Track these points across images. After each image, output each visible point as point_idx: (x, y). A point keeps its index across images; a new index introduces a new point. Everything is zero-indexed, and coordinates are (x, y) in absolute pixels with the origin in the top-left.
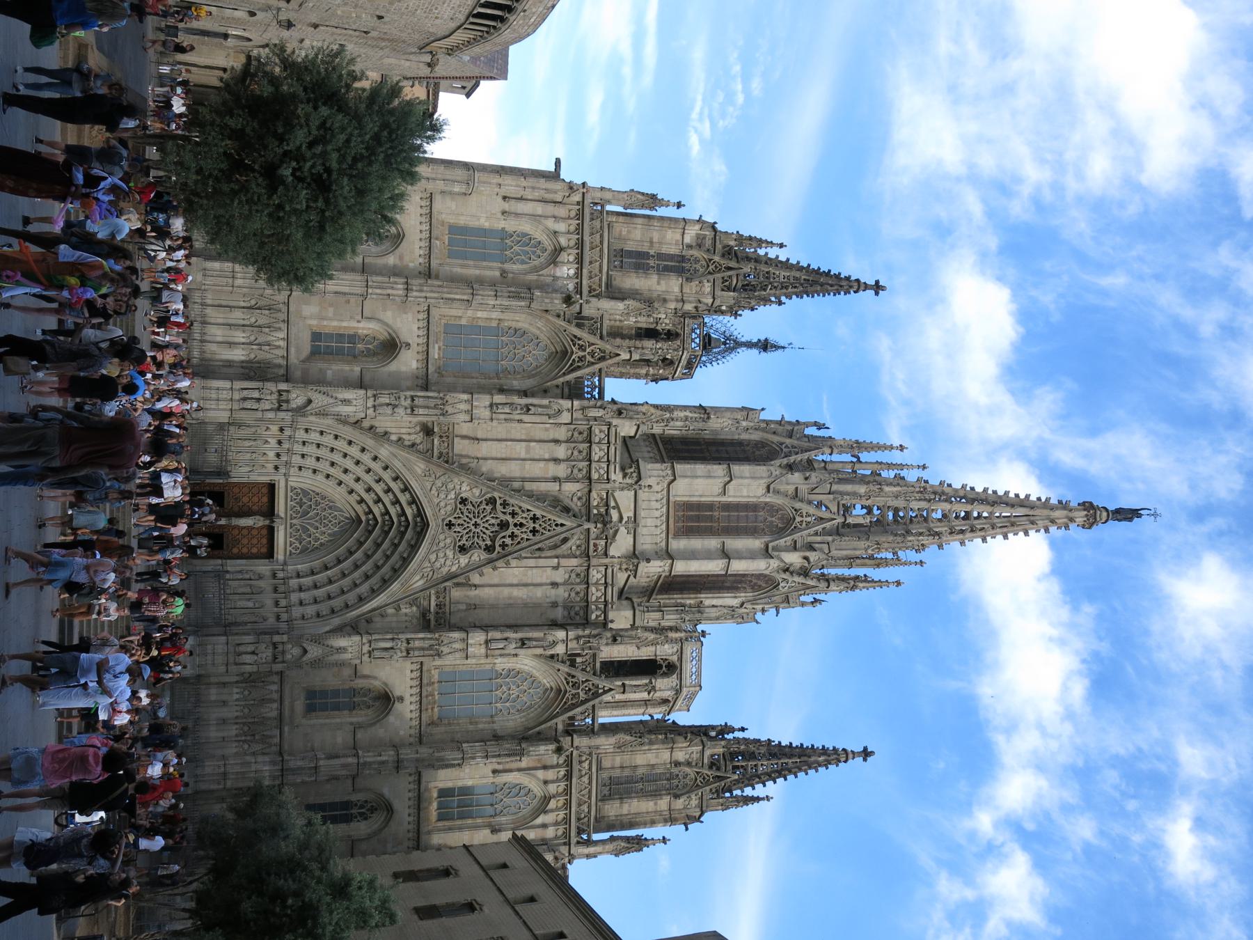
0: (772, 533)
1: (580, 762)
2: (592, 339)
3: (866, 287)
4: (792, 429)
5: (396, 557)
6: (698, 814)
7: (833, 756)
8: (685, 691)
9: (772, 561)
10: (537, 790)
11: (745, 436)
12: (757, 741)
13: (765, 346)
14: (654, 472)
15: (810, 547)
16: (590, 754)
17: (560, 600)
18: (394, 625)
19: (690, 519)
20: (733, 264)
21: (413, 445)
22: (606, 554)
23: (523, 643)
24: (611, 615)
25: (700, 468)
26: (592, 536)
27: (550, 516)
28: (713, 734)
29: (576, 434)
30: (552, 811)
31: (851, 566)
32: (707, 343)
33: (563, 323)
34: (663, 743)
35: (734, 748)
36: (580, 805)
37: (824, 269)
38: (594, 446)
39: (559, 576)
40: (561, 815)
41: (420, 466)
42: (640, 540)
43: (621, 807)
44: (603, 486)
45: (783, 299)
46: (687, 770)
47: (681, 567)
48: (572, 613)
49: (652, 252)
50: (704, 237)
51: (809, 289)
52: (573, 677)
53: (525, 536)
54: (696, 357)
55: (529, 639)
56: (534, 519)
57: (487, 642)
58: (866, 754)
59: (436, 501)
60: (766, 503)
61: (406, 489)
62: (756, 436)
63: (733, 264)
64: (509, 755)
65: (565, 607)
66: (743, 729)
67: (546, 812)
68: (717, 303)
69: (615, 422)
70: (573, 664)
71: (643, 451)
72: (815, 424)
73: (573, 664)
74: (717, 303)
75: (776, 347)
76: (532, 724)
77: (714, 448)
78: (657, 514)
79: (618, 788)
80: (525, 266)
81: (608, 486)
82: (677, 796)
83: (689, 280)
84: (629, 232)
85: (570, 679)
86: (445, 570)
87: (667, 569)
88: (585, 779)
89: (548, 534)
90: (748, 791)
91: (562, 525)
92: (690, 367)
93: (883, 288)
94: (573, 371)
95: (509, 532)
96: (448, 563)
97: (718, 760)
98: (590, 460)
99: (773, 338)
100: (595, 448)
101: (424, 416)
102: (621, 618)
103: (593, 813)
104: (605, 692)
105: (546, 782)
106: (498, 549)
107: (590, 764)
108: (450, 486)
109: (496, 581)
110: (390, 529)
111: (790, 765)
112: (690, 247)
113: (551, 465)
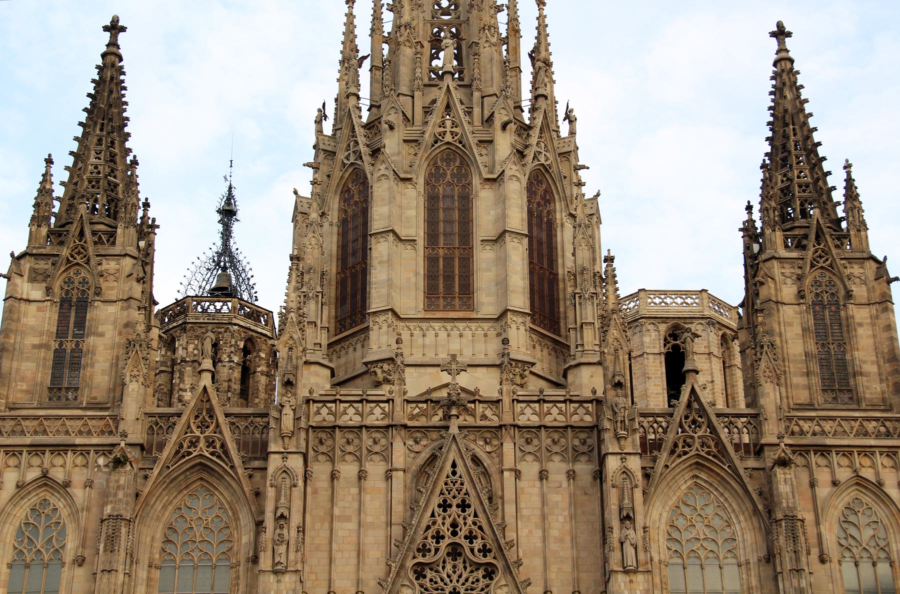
0: (467, 175)
1: (802, 433)
2: (178, 428)
3: (113, 43)
4: (325, 152)
6: (874, 265)
7: (785, 76)
8: (707, 313)
9: (508, 173)
10: (847, 497)
11: (334, 216)
12: (766, 184)
13: (228, 213)
14: (380, 341)
15: (489, 121)
16: (790, 419)
17: (564, 467)
19: (449, 289)
20: (74, 229)
22: (498, 401)
23: (627, 518)
24: (587, 394)
25: (378, 275)
26: (470, 421)
27: (441, 484)
28: (756, 248)
29: (323, 449)
30: (877, 474)
31: (518, 70)
32: (223, 292)
33: (156, 471)
34: (770, 315)
35: (775, 216)
36: (866, 434)
37: (87, 103)
38: (340, 422)
39: (530, 468)
40: (879, 459)
42: (481, 359)
43: (867, 375)
44: (398, 408)
45: (129, 159)
46: (808, 281)
47: (520, 300)
48: (585, 449)
49: (54, 345)
50: (33, 270)
51: (116, 123)
52: (676, 445)
53: (470, 520)
54: (242, 308)
55: (621, 510)
56: (445, 506)
57: (626, 572)
58: (781, 33)
60: (427, 183)
62: (334, 204)
63: (74, 229)
64: (795, 539)
65: (575, 460)
66: (749, 208)
67: (880, 485)
68: (135, 252)
69: (303, 392)
70: (657, 445)
71: (353, 359)
72: (319, 122)
73: (657, 445)
74: (135, 252)
75: (230, 198)
76: (749, 505)
77: (351, 261)
78: (443, 334)
79: (837, 378)
80: (70, 529)
81: (398, 401)
82: (849, 295)
83: (98, 292)
84: (23, 379)
85: (680, 450)
87: (520, 320)
88: (828, 426)
89: (467, 486)
90: (838, 196)
91: (454, 465)
92: (256, 314)
93: (115, 22)
94: (226, 452)
95: (465, 544)
97: (794, 237)
98: (361, 427)
99: (218, 202)
100: (343, 421)
102: (589, 381)
103: (878, 414)
104: (698, 399)
105: (835, 483)
107: (805, 419)
109: (538, 562)
111: (799, 137)
112: (48, 290)
113: (368, 484)
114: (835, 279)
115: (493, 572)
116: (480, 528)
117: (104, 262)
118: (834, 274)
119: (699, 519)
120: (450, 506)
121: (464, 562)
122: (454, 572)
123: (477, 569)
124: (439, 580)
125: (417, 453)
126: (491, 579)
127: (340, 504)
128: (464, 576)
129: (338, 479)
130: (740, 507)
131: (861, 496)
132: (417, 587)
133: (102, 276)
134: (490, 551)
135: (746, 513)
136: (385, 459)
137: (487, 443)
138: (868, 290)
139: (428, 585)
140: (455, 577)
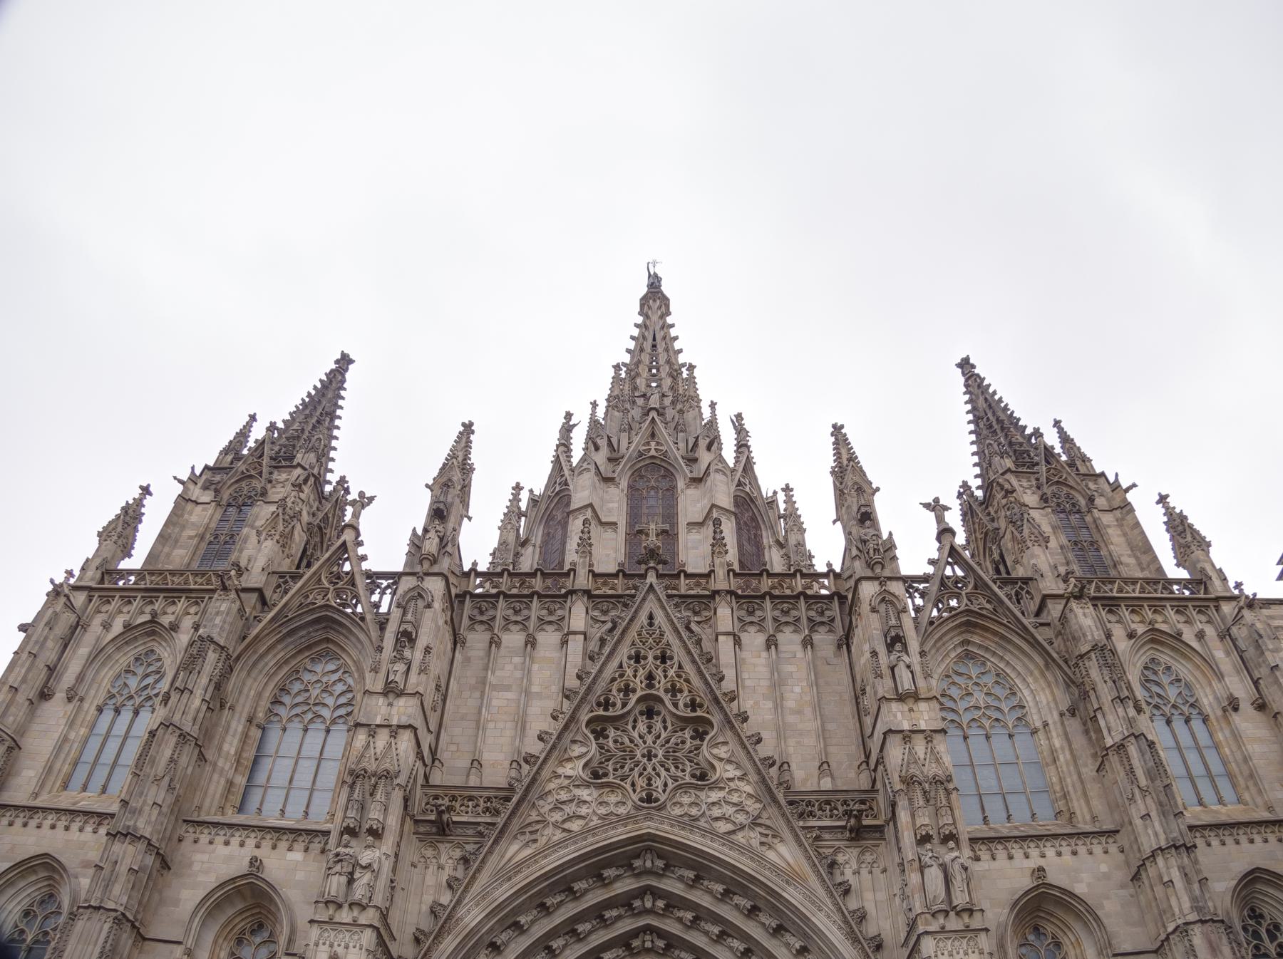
5: (725, 911)
9: (713, 468)
18: (881, 896)
21: (465, 861)
39: (754, 639)
41: (514, 850)
53: (671, 673)
56: (637, 658)
59: (596, 821)
61: (563, 882)
65: (812, 630)
82: (1091, 500)
86: (753, 807)
95: (667, 699)
96: (735, 798)
101: (387, 812)
106: (699, 713)
108: (564, 796)
110: (661, 934)
114: (1072, 492)
115: (707, 733)
116: (687, 681)
117: (276, 473)
118: (1072, 487)
119: (976, 688)
120: (645, 658)
121: (664, 721)
122: (650, 732)
123: (682, 730)
124: (626, 740)
125: (603, 622)
126: (702, 740)
127: (498, 673)
128: (664, 735)
129: (498, 645)
130: (1027, 668)
131: (1158, 655)
132: (594, 746)
133: (270, 482)
134: (701, 706)
135: (1036, 673)
136: (560, 629)
137: (696, 613)
138: (1108, 500)
139: (611, 744)
140: (649, 739)
